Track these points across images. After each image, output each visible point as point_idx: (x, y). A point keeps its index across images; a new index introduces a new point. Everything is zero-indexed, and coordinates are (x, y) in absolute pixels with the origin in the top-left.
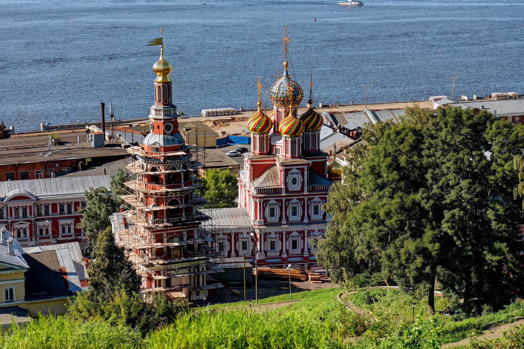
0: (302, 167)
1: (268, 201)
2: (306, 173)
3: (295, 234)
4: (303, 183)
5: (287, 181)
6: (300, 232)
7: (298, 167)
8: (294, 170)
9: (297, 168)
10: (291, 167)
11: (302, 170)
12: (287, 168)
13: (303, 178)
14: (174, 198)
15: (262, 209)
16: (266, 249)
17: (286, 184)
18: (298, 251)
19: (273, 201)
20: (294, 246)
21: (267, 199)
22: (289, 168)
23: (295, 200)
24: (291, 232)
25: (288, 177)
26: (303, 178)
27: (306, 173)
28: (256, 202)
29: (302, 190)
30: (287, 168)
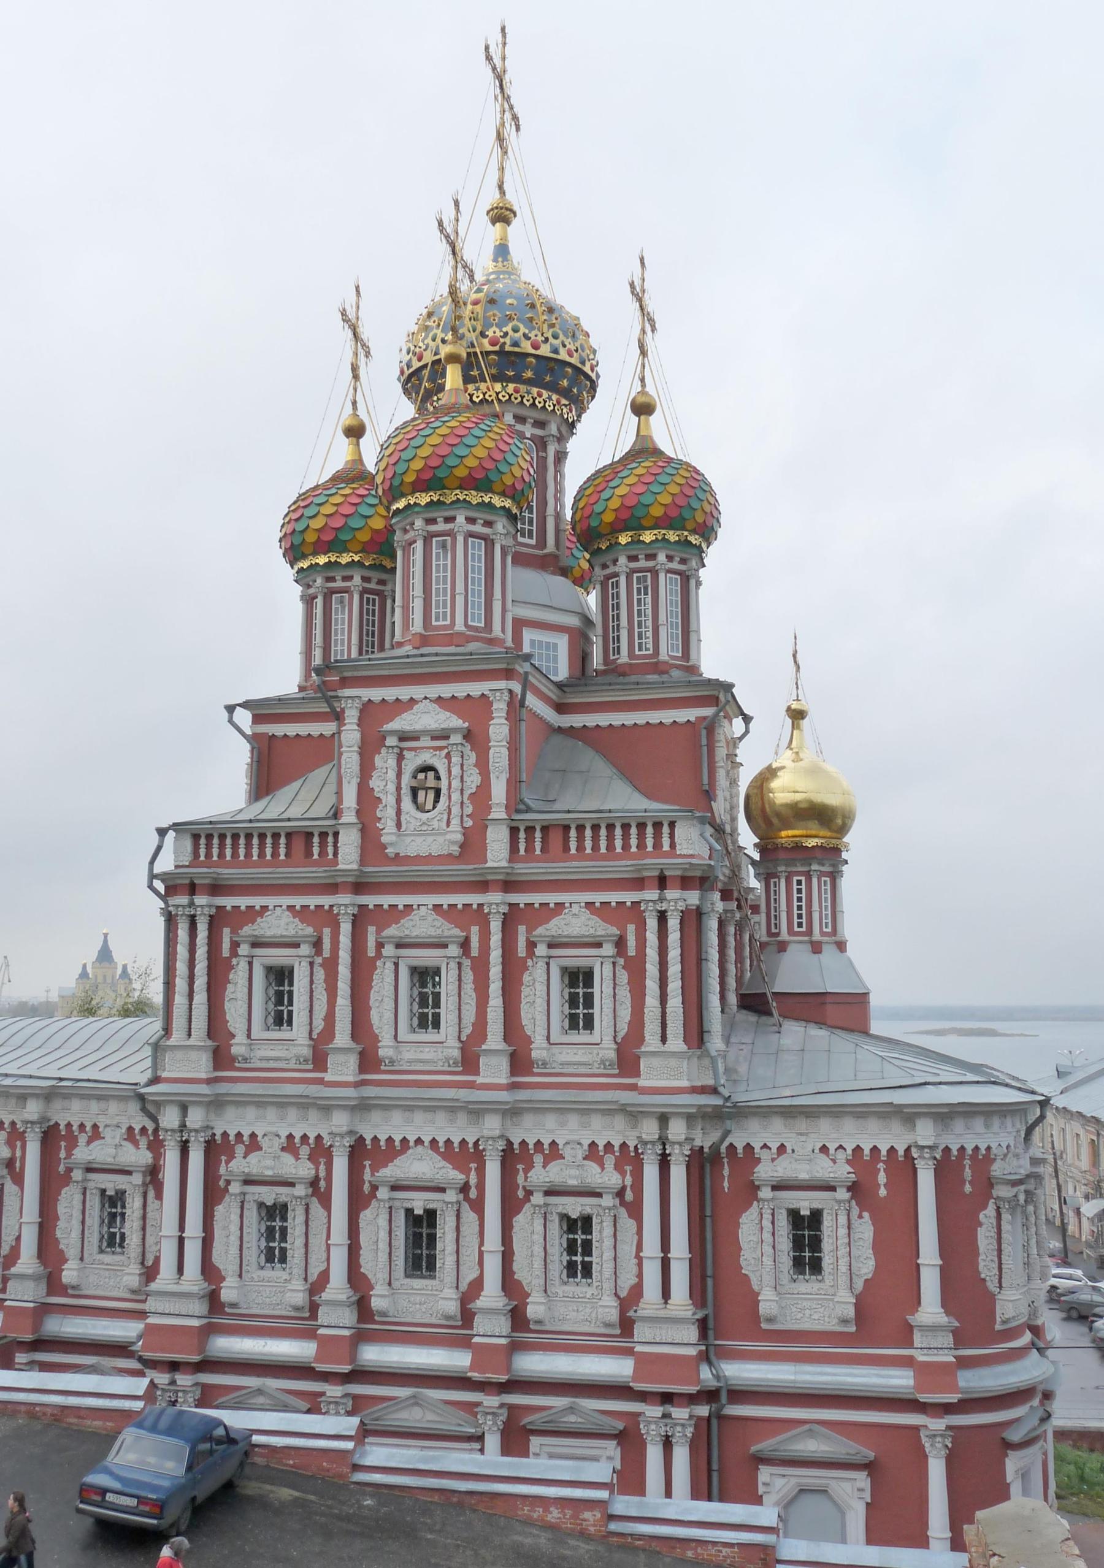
0: (476, 689)
1: (253, 914)
2: (499, 730)
5: (375, 783)
9: (439, 700)
10: (404, 692)
12: (376, 694)
15: (201, 967)
17: (367, 799)
18: (433, 1298)
19: (278, 919)
20: (421, 1251)
22: (390, 693)
23: (423, 918)
24: (393, 1150)
25: (378, 760)
27: (499, 730)
30: (376, 694)
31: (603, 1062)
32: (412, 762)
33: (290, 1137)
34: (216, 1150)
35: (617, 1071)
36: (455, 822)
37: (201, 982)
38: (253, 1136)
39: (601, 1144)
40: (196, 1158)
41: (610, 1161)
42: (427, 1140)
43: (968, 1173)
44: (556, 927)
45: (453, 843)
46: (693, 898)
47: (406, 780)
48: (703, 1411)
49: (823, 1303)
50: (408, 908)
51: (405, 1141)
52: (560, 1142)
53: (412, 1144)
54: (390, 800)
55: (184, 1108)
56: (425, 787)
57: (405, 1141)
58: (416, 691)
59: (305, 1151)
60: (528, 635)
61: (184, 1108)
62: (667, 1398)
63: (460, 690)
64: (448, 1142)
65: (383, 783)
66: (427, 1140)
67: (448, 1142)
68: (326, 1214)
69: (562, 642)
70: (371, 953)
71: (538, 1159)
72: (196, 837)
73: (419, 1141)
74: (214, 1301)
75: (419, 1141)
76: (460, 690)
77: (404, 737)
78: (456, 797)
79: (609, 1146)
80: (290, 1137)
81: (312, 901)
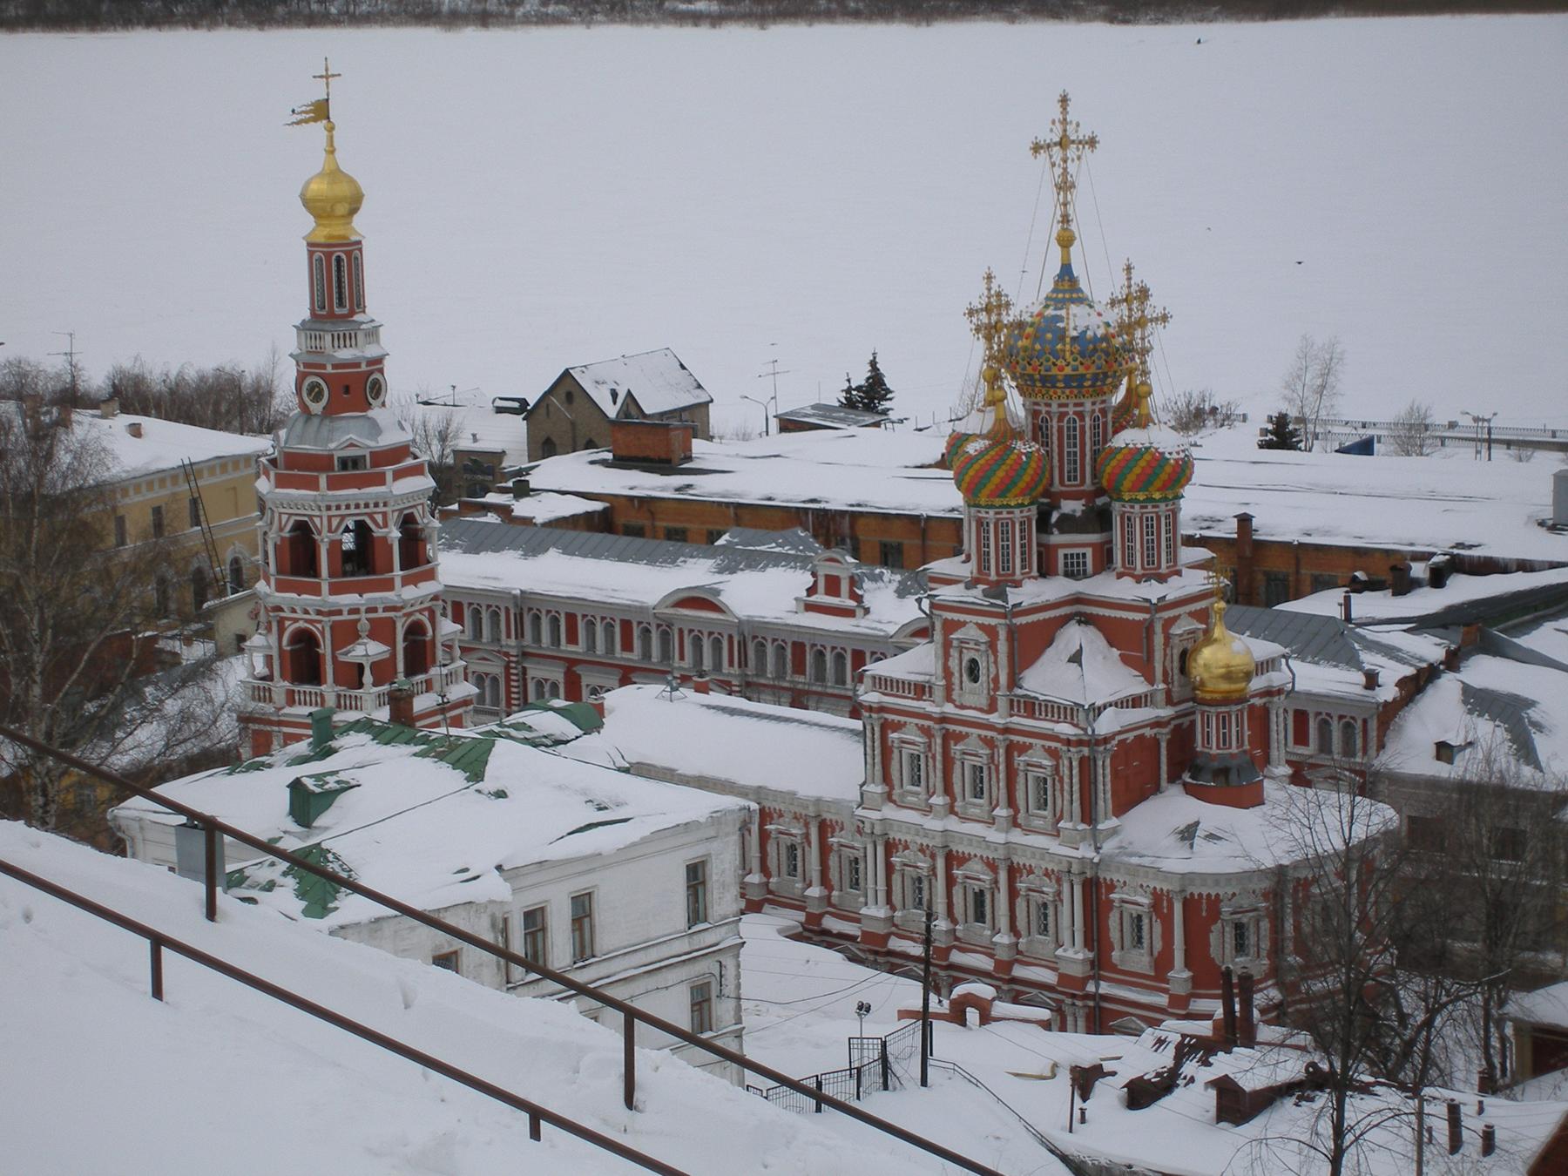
0: (993, 621)
8: (971, 632)
11: (991, 631)
14: (301, 624)
17: (947, 674)
27: (1002, 646)
32: (967, 656)
40: (880, 850)
43: (1204, 907)
46: (1086, 751)
48: (1091, 1004)
49: (1140, 961)
50: (967, 735)
54: (957, 675)
60: (1061, 552)
62: (1074, 996)
65: (954, 664)
69: (1089, 552)
77: (962, 641)
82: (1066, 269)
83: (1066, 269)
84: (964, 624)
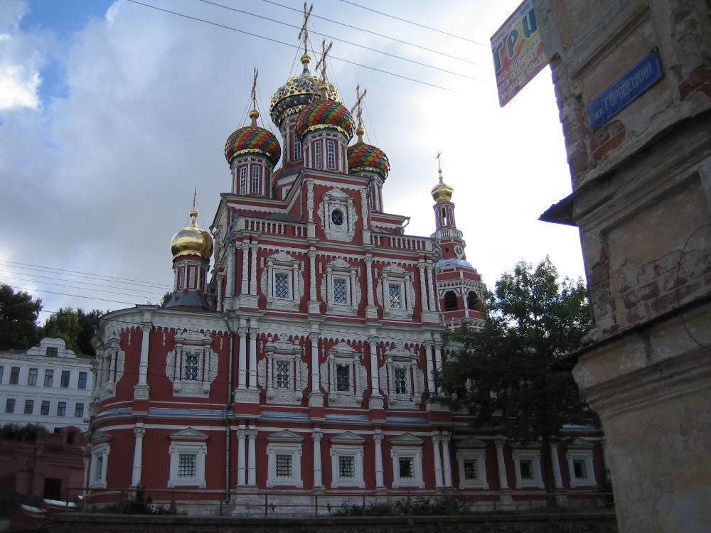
1: (271, 252)
3: (343, 348)
4: (359, 224)
5: (320, 213)
6: (354, 344)
7: (346, 186)
9: (342, 189)
10: (329, 184)
12: (318, 182)
13: (359, 212)
15: (254, 268)
16: (262, 381)
21: (268, 247)
26: (359, 212)
28: (238, 254)
29: (358, 238)
30: (318, 182)
31: (408, 316)
33: (291, 336)
34: (262, 339)
35: (411, 320)
36: (351, 230)
37: (254, 274)
38: (276, 335)
39: (409, 344)
41: (412, 349)
42: (346, 340)
44: (388, 268)
45: (350, 236)
47: (331, 214)
51: (337, 340)
52: (396, 343)
53: (340, 340)
55: (248, 320)
56: (337, 218)
57: (337, 340)
58: (334, 184)
59: (297, 342)
61: (248, 320)
63: (352, 187)
64: (354, 341)
66: (346, 340)
67: (354, 341)
68: (306, 365)
70: (321, 272)
71: (388, 348)
72: (247, 222)
73: (343, 340)
74: (263, 396)
75: (343, 340)
76: (352, 187)
78: (350, 221)
79: (412, 345)
80: (291, 336)
81: (297, 250)
82: (306, 70)
83: (306, 70)
84: (331, 188)
